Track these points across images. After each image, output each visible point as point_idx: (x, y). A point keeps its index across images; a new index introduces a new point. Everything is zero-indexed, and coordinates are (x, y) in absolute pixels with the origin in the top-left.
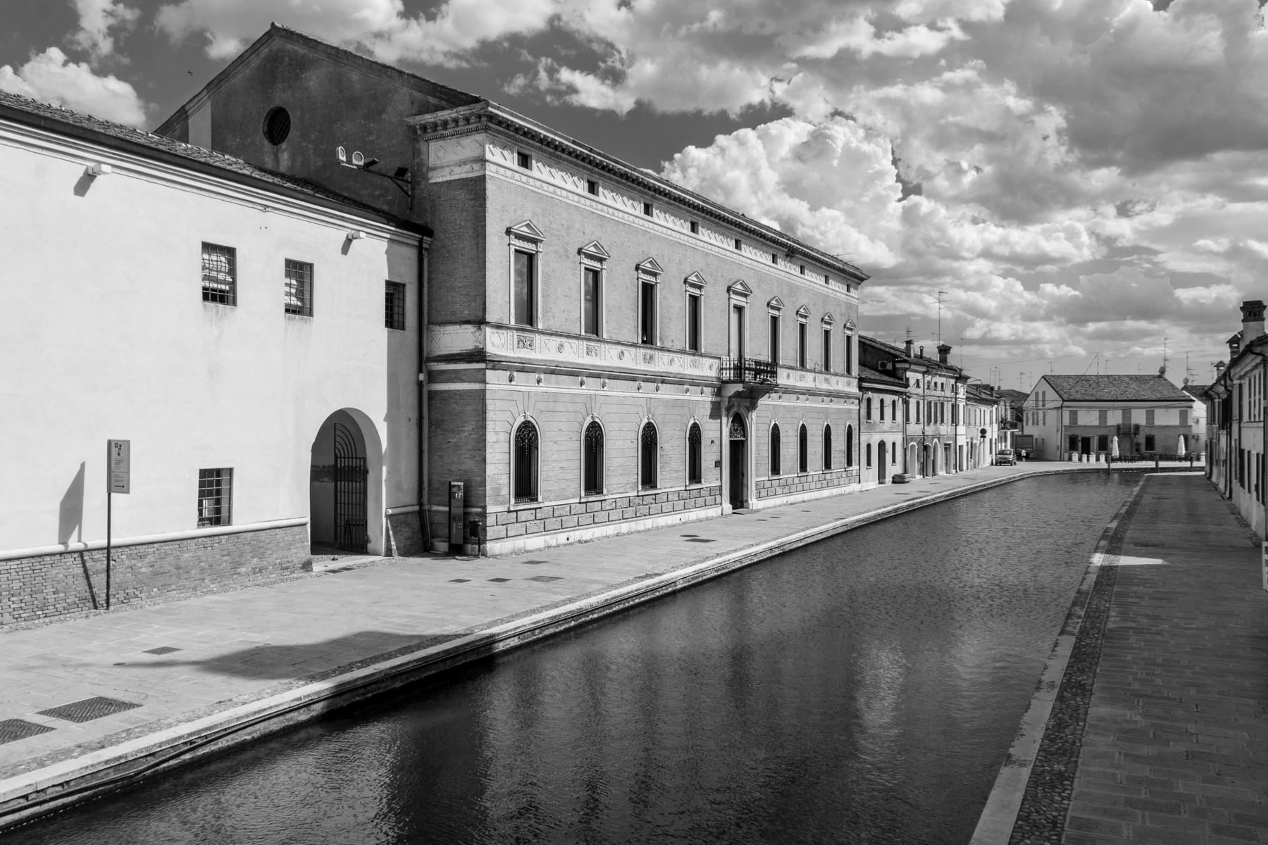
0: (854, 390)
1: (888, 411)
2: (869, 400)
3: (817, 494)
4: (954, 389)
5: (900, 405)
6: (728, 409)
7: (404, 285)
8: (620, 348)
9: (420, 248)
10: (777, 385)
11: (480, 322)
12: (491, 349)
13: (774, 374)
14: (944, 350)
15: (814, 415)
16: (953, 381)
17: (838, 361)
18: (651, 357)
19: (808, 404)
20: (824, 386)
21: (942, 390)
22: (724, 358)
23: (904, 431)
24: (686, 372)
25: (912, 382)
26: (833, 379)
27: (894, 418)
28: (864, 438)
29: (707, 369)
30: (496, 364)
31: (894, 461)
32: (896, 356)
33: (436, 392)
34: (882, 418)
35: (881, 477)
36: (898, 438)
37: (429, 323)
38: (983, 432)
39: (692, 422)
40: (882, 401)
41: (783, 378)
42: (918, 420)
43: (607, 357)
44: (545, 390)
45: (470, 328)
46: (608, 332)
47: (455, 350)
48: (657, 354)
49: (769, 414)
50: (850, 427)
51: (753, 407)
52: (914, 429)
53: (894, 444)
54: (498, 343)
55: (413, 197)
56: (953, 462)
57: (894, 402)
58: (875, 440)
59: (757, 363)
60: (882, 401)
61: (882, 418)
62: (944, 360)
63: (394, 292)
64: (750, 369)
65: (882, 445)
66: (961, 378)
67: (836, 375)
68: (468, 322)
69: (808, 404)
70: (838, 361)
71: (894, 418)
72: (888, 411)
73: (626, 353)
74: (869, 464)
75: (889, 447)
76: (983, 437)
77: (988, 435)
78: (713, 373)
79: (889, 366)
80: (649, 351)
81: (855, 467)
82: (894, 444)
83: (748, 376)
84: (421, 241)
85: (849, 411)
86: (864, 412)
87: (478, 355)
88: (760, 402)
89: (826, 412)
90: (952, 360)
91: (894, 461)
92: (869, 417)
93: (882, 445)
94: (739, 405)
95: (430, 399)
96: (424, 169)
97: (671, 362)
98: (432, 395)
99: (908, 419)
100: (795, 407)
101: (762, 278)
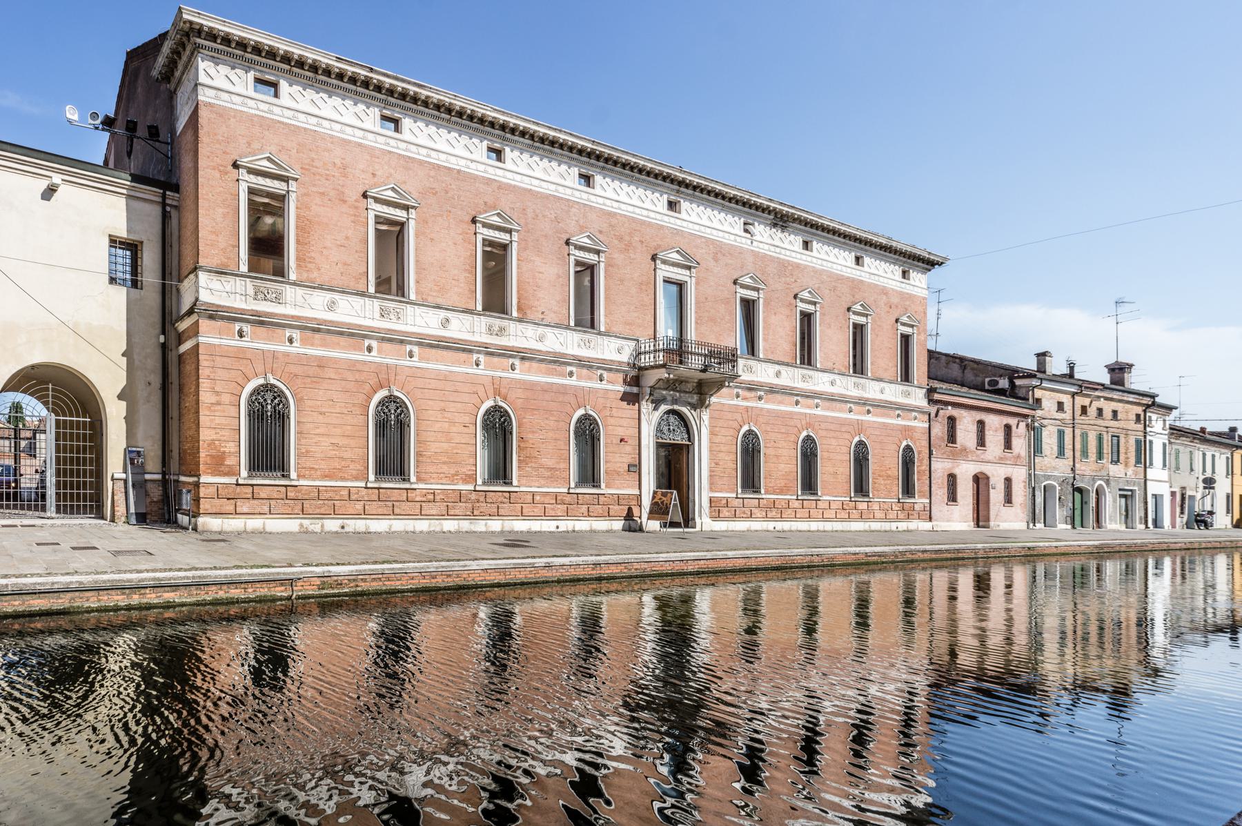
1: (995, 438)
5: (1020, 430)
15: (832, 427)
16: (1139, 410)
19: (819, 412)
20: (854, 393)
21: (1100, 411)
23: (1031, 466)
27: (1008, 445)
28: (941, 467)
31: (1008, 500)
34: (981, 442)
36: (1019, 475)
42: (1061, 453)
50: (908, 449)
52: (1053, 467)
53: (1008, 481)
56: (1139, 513)
58: (965, 471)
61: (981, 442)
65: (980, 481)
67: (881, 380)
69: (819, 412)
71: (1008, 445)
72: (995, 438)
74: (952, 497)
81: (920, 501)
82: (1008, 481)
85: (907, 430)
86: (939, 430)
89: (860, 427)
91: (1008, 500)
92: (952, 438)
93: (980, 481)
99: (1036, 448)
100: (791, 413)
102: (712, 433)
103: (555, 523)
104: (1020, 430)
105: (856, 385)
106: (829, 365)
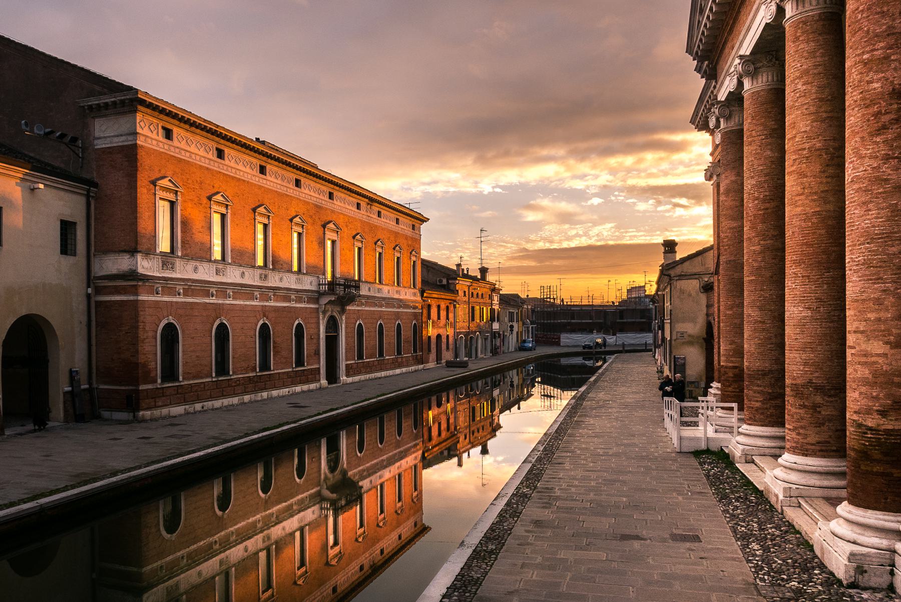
0: (419, 298)
2: (429, 306)
3: (390, 373)
4: (491, 297)
6: (324, 312)
7: (75, 224)
8: (242, 269)
9: (88, 197)
10: (360, 296)
11: (133, 251)
12: (141, 270)
13: (357, 287)
14: (484, 271)
17: (406, 277)
18: (266, 276)
22: (321, 276)
24: (292, 287)
25: (461, 293)
26: (403, 291)
27: (448, 318)
29: (308, 283)
30: (145, 278)
31: (448, 348)
32: (449, 275)
33: (101, 302)
34: (439, 318)
35: (439, 358)
37: (95, 250)
38: (512, 327)
39: (297, 322)
40: (439, 307)
41: (364, 291)
43: (233, 275)
44: (183, 300)
45: (126, 257)
46: (232, 258)
47: (115, 272)
48: (271, 274)
49: (355, 316)
51: (343, 311)
54: (145, 266)
55: (83, 158)
57: (447, 307)
59: (346, 279)
60: (439, 307)
61: (439, 318)
62: (483, 277)
63: (67, 227)
64: (340, 285)
66: (494, 290)
68: (125, 251)
70: (406, 277)
71: (448, 318)
72: (443, 314)
73: (246, 273)
75: (444, 340)
76: (512, 330)
77: (515, 329)
78: (314, 288)
79: (445, 282)
80: (264, 272)
83: (340, 291)
84: (88, 191)
87: (133, 275)
88: (348, 308)
90: (490, 278)
91: (448, 348)
94: (332, 311)
95: (96, 307)
96: (92, 138)
97: (281, 279)
98: (98, 304)
101: (350, 220)
102: (346, 327)
103: (287, 390)
104: (451, 308)
105: (397, 292)
106: (387, 282)
